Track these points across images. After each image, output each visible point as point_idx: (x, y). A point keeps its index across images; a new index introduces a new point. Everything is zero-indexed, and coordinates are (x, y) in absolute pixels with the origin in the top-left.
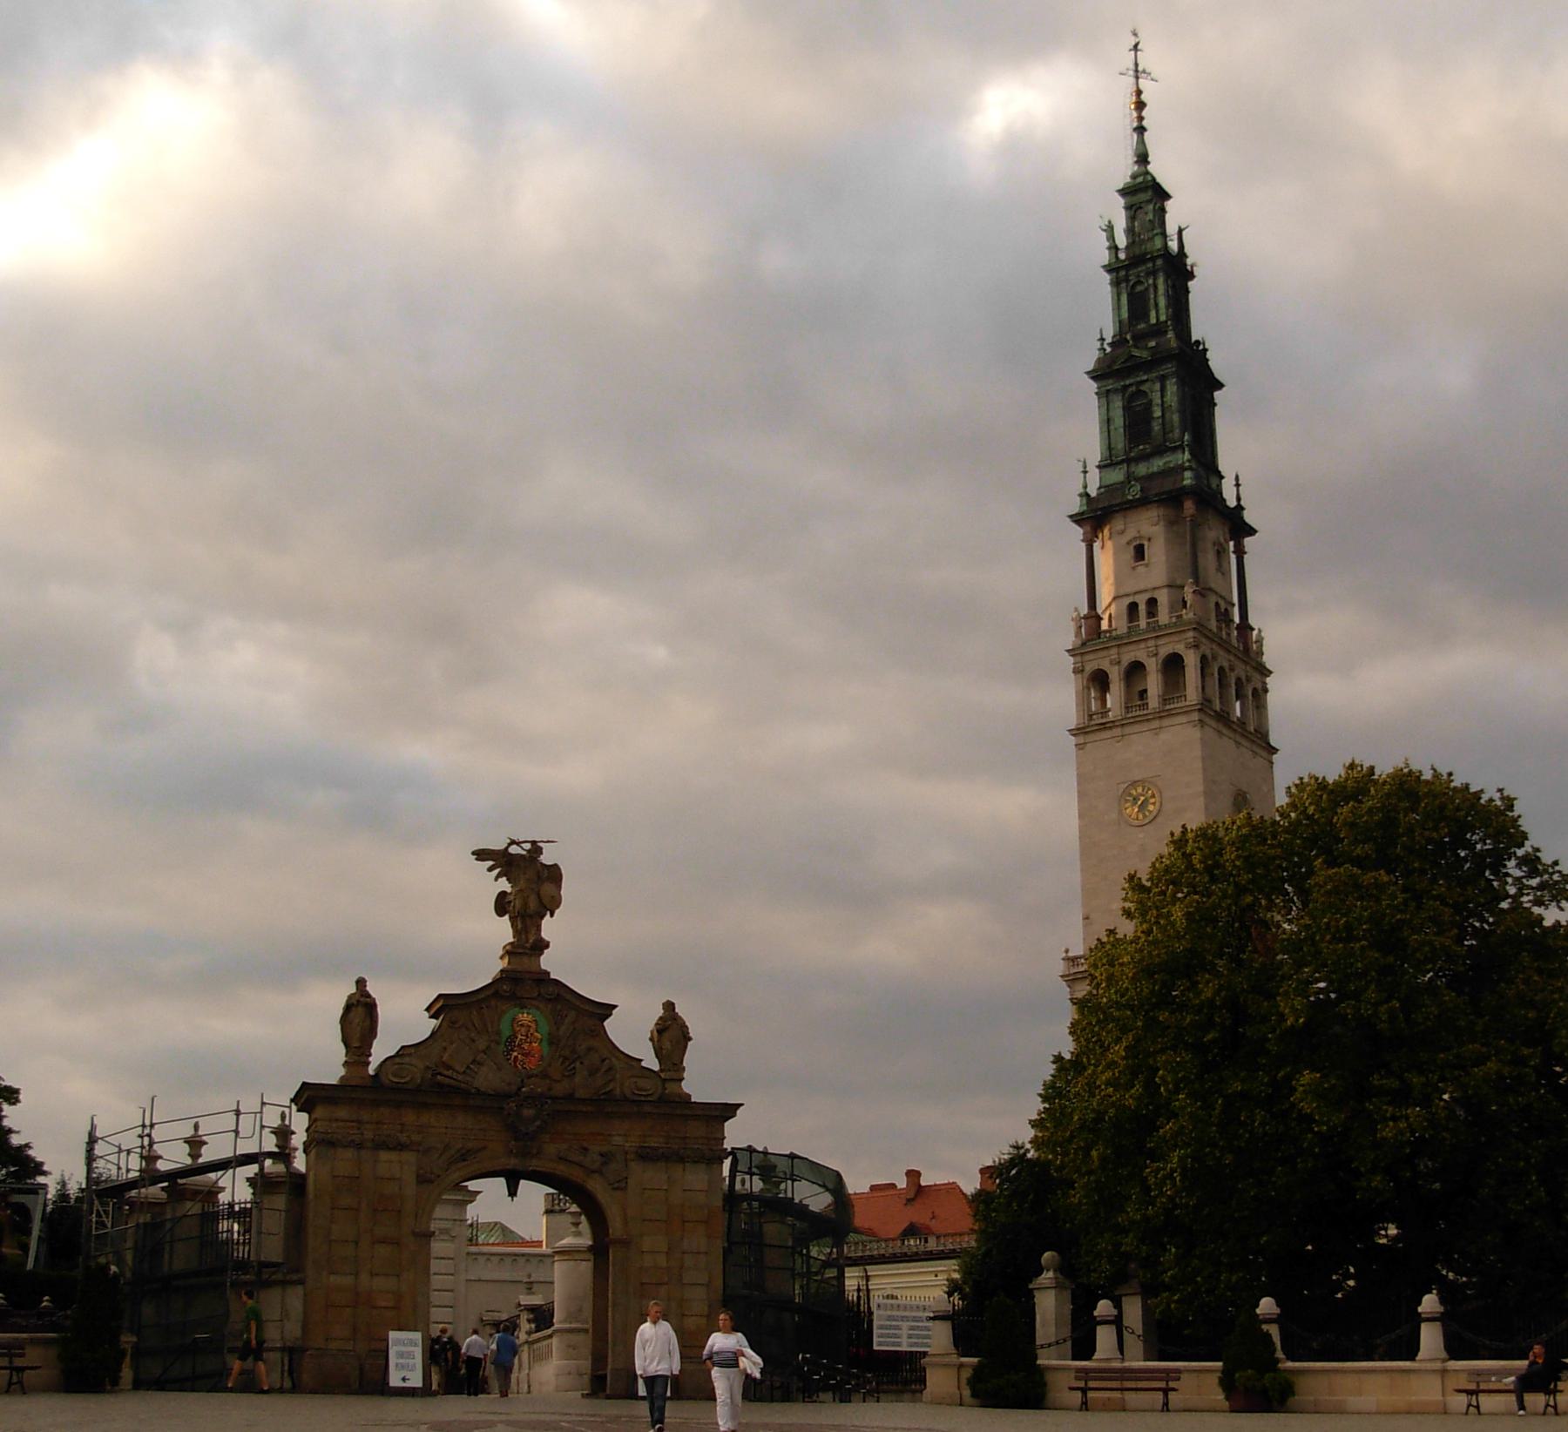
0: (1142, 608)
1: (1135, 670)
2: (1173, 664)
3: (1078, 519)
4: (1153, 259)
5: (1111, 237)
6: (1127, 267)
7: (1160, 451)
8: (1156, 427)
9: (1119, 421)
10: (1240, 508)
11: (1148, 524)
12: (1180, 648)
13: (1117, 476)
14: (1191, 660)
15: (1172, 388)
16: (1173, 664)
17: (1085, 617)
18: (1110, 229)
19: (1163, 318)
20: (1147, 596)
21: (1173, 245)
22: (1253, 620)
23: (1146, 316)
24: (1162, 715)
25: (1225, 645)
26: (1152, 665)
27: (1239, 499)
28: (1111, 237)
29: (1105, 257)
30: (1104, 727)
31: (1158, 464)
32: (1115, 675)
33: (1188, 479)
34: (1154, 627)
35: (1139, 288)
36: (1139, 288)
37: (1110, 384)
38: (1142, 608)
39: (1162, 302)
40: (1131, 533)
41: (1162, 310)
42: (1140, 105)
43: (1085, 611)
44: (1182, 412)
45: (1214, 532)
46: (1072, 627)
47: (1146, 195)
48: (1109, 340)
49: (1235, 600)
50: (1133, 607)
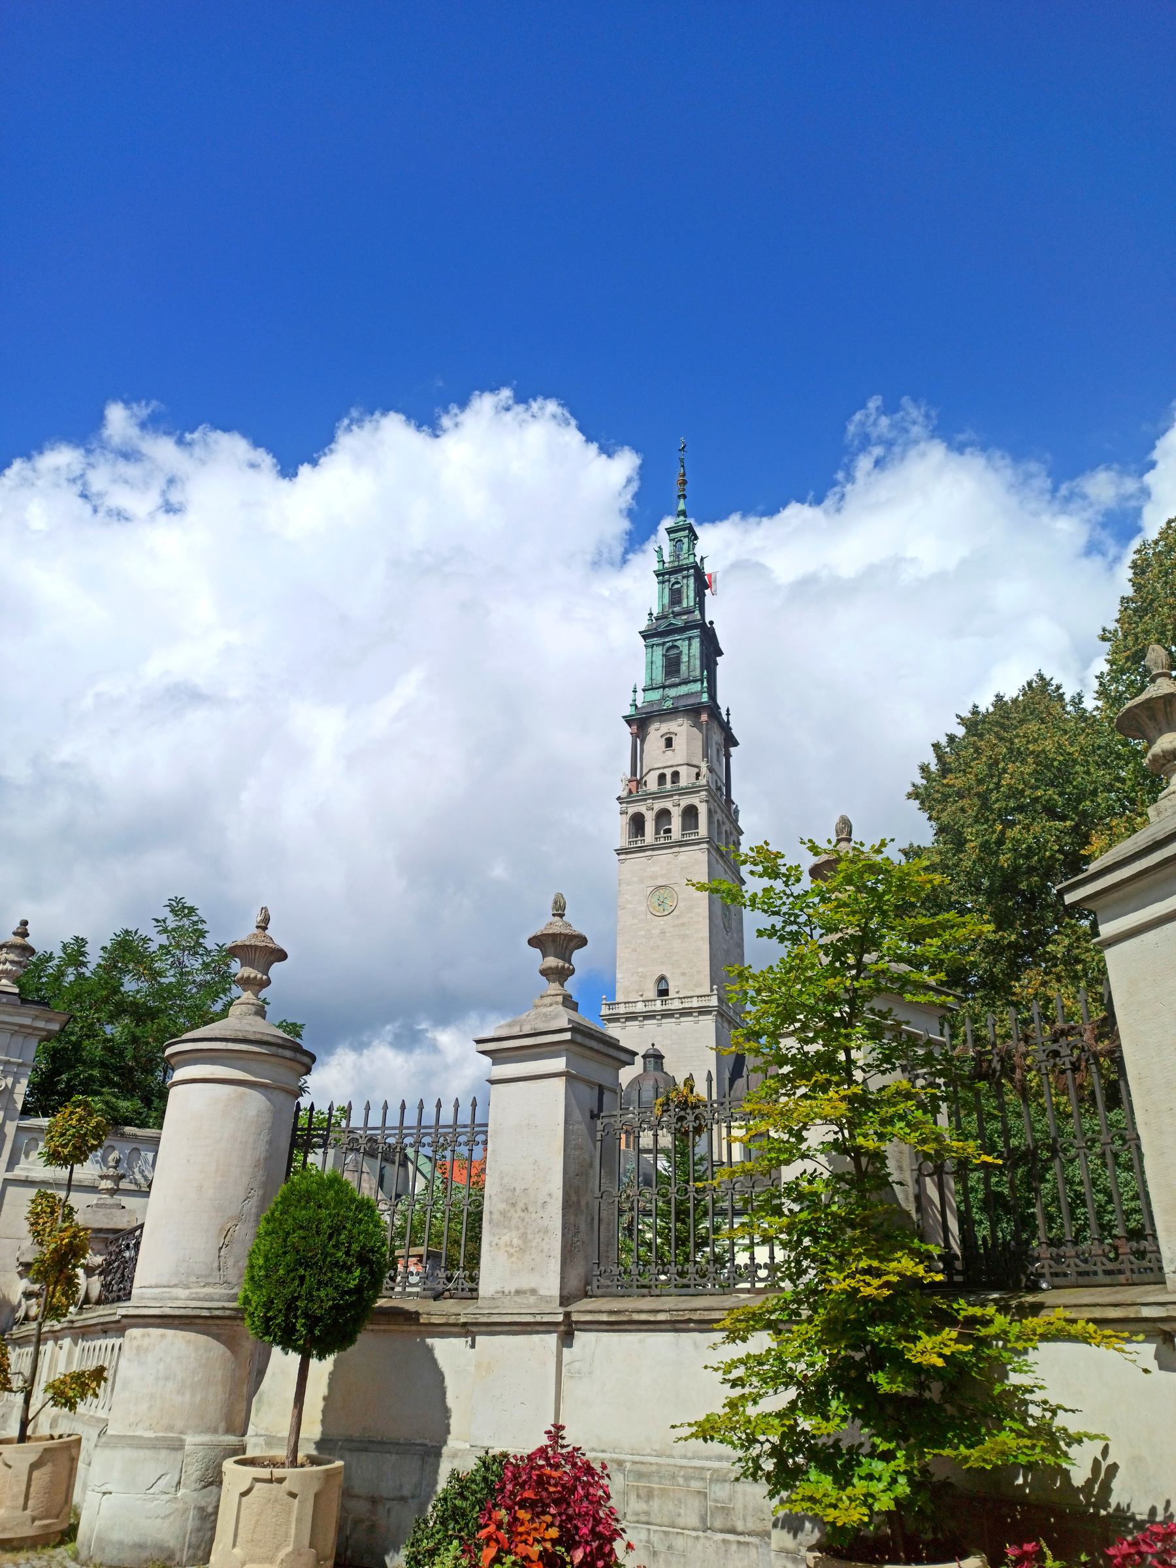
2: (690, 813)
3: (629, 720)
4: (688, 569)
7: (686, 682)
8: (683, 668)
13: (655, 695)
14: (703, 810)
15: (696, 643)
16: (690, 813)
22: (733, 797)
23: (679, 602)
24: (681, 844)
30: (642, 849)
31: (683, 690)
35: (676, 586)
36: (676, 586)
39: (692, 594)
42: (684, 482)
50: (662, 777)
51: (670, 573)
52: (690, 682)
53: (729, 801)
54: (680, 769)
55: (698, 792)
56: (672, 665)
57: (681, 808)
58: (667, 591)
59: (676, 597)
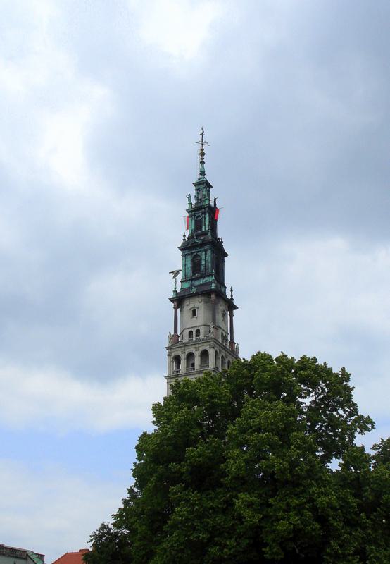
0: (194, 333)
1: (191, 355)
2: (205, 354)
3: (172, 300)
4: (205, 208)
5: (190, 200)
6: (195, 211)
7: (203, 277)
8: (203, 268)
9: (189, 265)
10: (232, 299)
11: (198, 303)
12: (207, 348)
13: (187, 285)
14: (211, 352)
15: (209, 254)
16: (205, 354)
17: (173, 336)
18: (189, 198)
19: (207, 229)
20: (196, 329)
21: (212, 204)
23: (201, 228)
25: (224, 348)
26: (197, 354)
27: (232, 296)
28: (190, 200)
29: (187, 207)
31: (202, 281)
32: (183, 357)
33: (213, 286)
34: (198, 340)
37: (187, 252)
38: (194, 333)
39: (207, 223)
40: (191, 306)
41: (207, 226)
42: (203, 154)
43: (173, 333)
44: (212, 262)
45: (222, 307)
46: (167, 339)
47: (203, 186)
48: (187, 236)
49: (229, 332)
50: (191, 333)
53: (232, 342)
54: (199, 328)
57: (200, 352)
58: (194, 221)
59: (198, 225)
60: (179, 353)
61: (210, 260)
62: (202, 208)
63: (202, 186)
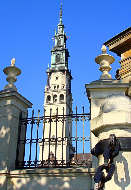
2: (62, 96)
4: (62, 35)
6: (58, 36)
8: (61, 60)
15: (64, 54)
19: (63, 44)
23: (60, 44)
31: (60, 65)
36: (59, 39)
38: (57, 87)
40: (56, 75)
50: (55, 87)
51: (58, 36)
52: (62, 64)
54: (59, 85)
55: (64, 91)
56: (58, 59)
58: (57, 40)
60: (50, 95)
61: (64, 57)
62: (61, 36)
63: (61, 26)
